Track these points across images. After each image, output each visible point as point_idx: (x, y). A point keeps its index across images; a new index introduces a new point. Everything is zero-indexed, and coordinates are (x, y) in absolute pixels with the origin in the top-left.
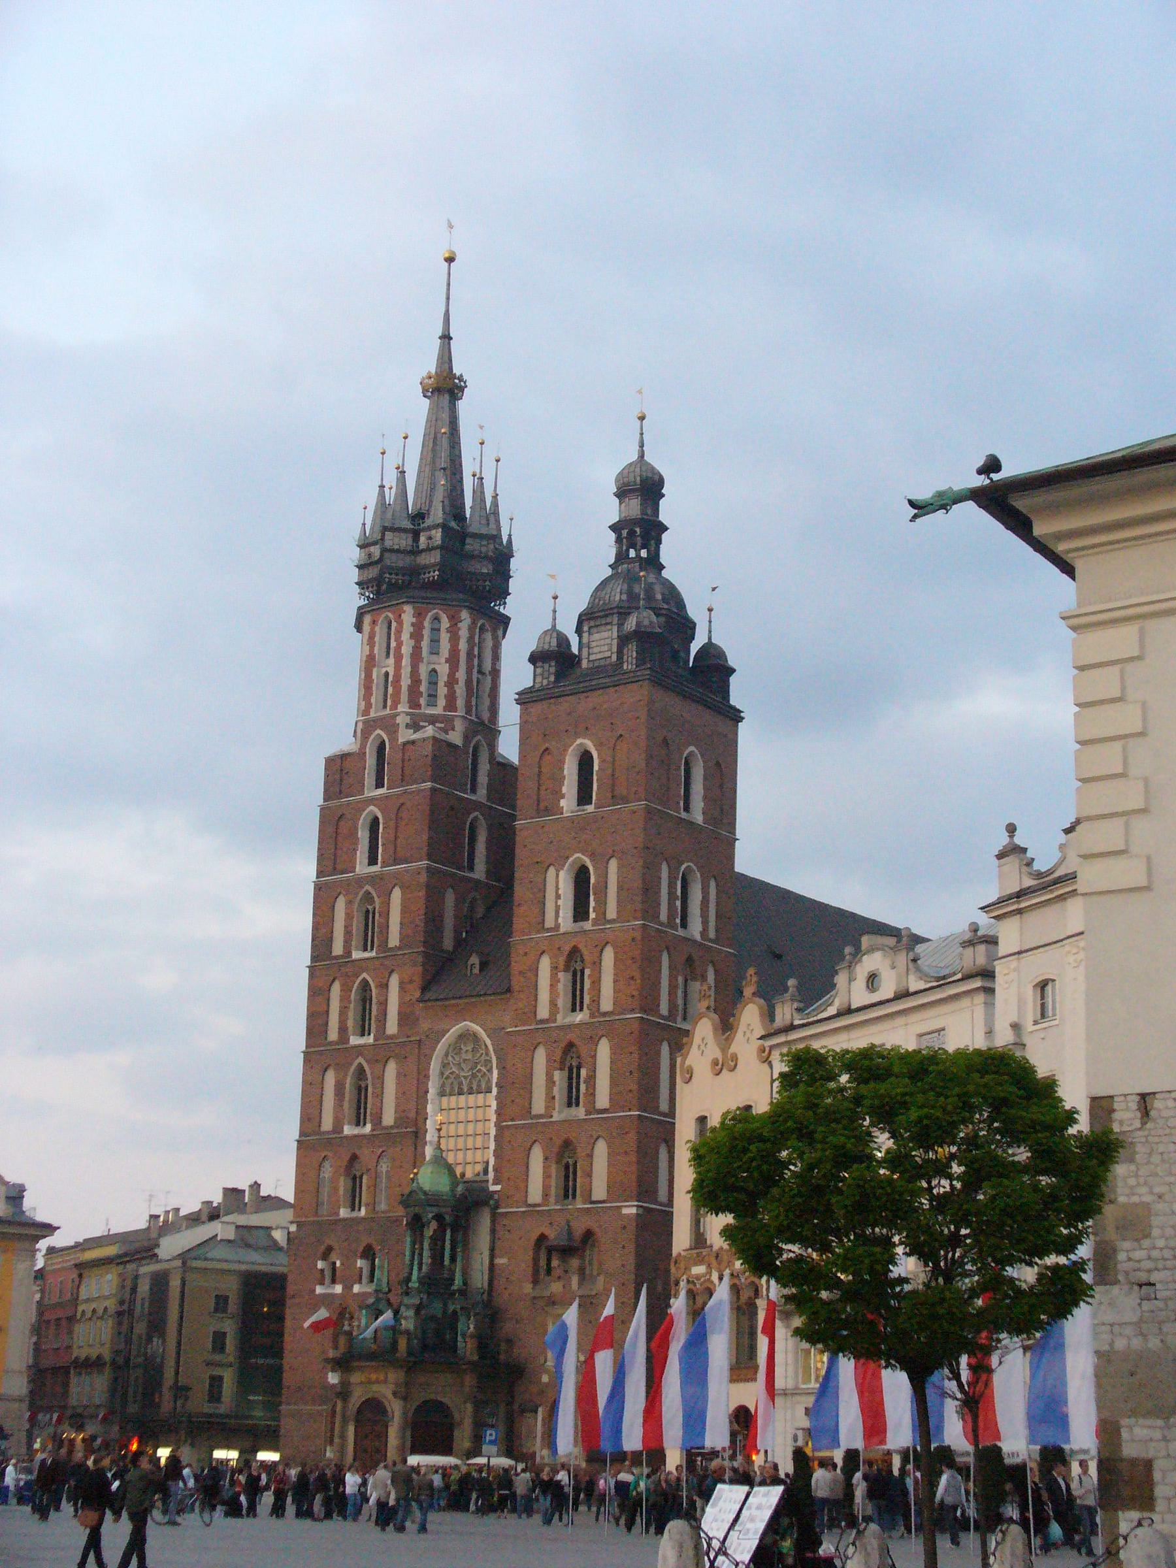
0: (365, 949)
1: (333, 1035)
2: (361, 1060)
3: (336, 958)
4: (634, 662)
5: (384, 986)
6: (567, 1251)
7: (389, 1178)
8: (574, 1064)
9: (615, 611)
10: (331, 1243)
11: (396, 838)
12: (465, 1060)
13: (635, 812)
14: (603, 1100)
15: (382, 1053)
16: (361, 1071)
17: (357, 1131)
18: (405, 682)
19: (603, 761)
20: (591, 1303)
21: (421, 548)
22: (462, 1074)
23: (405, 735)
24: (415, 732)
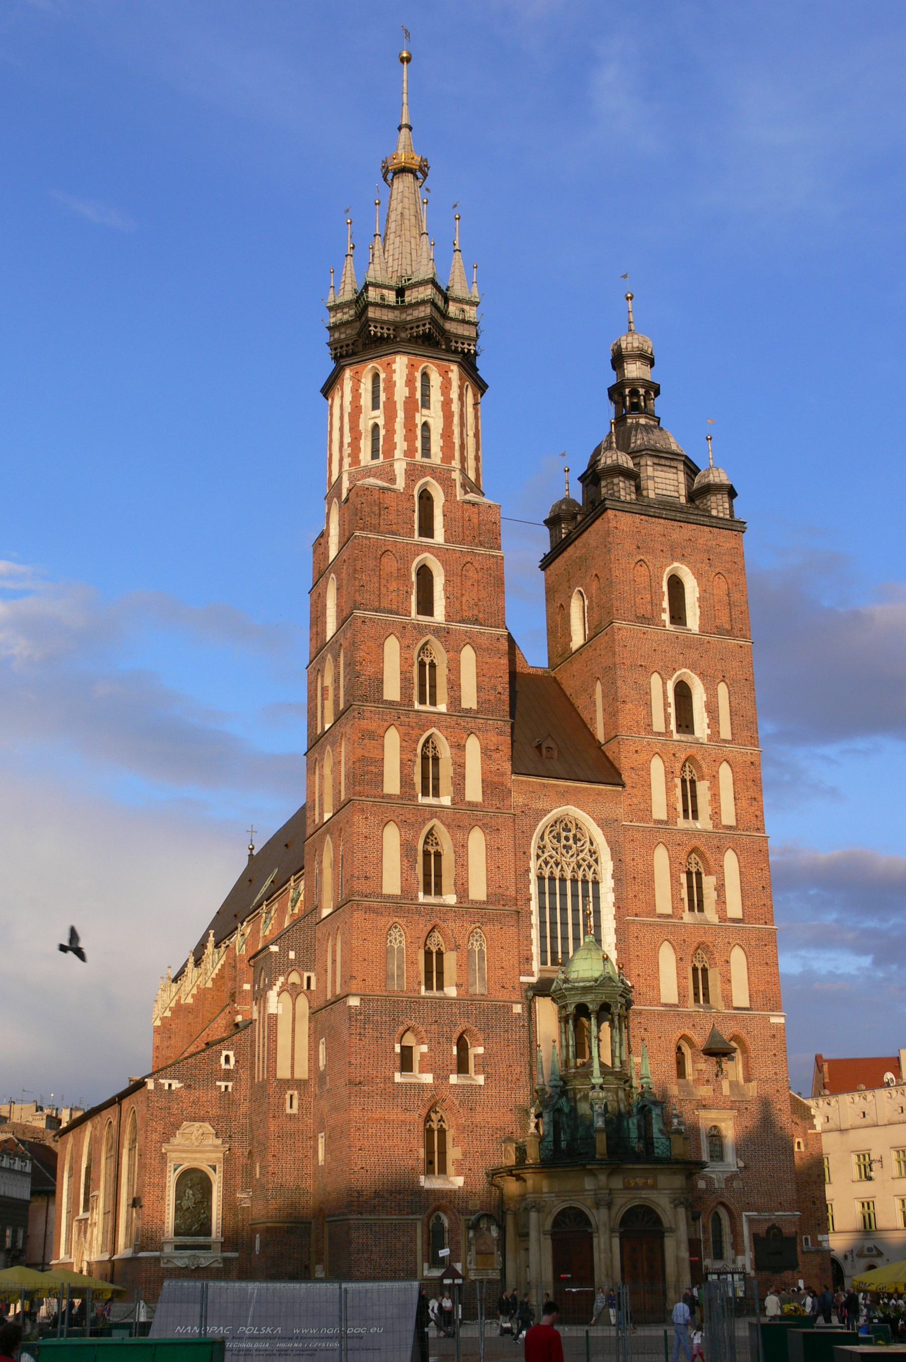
0: (422, 701)
1: (392, 785)
2: (435, 821)
3: (391, 703)
5: (459, 747)
7: (482, 959)
8: (694, 870)
9: (683, 458)
12: (565, 847)
13: (741, 647)
14: (734, 909)
18: (457, 440)
19: (703, 591)
20: (746, 1108)
21: (452, 315)
22: (563, 859)
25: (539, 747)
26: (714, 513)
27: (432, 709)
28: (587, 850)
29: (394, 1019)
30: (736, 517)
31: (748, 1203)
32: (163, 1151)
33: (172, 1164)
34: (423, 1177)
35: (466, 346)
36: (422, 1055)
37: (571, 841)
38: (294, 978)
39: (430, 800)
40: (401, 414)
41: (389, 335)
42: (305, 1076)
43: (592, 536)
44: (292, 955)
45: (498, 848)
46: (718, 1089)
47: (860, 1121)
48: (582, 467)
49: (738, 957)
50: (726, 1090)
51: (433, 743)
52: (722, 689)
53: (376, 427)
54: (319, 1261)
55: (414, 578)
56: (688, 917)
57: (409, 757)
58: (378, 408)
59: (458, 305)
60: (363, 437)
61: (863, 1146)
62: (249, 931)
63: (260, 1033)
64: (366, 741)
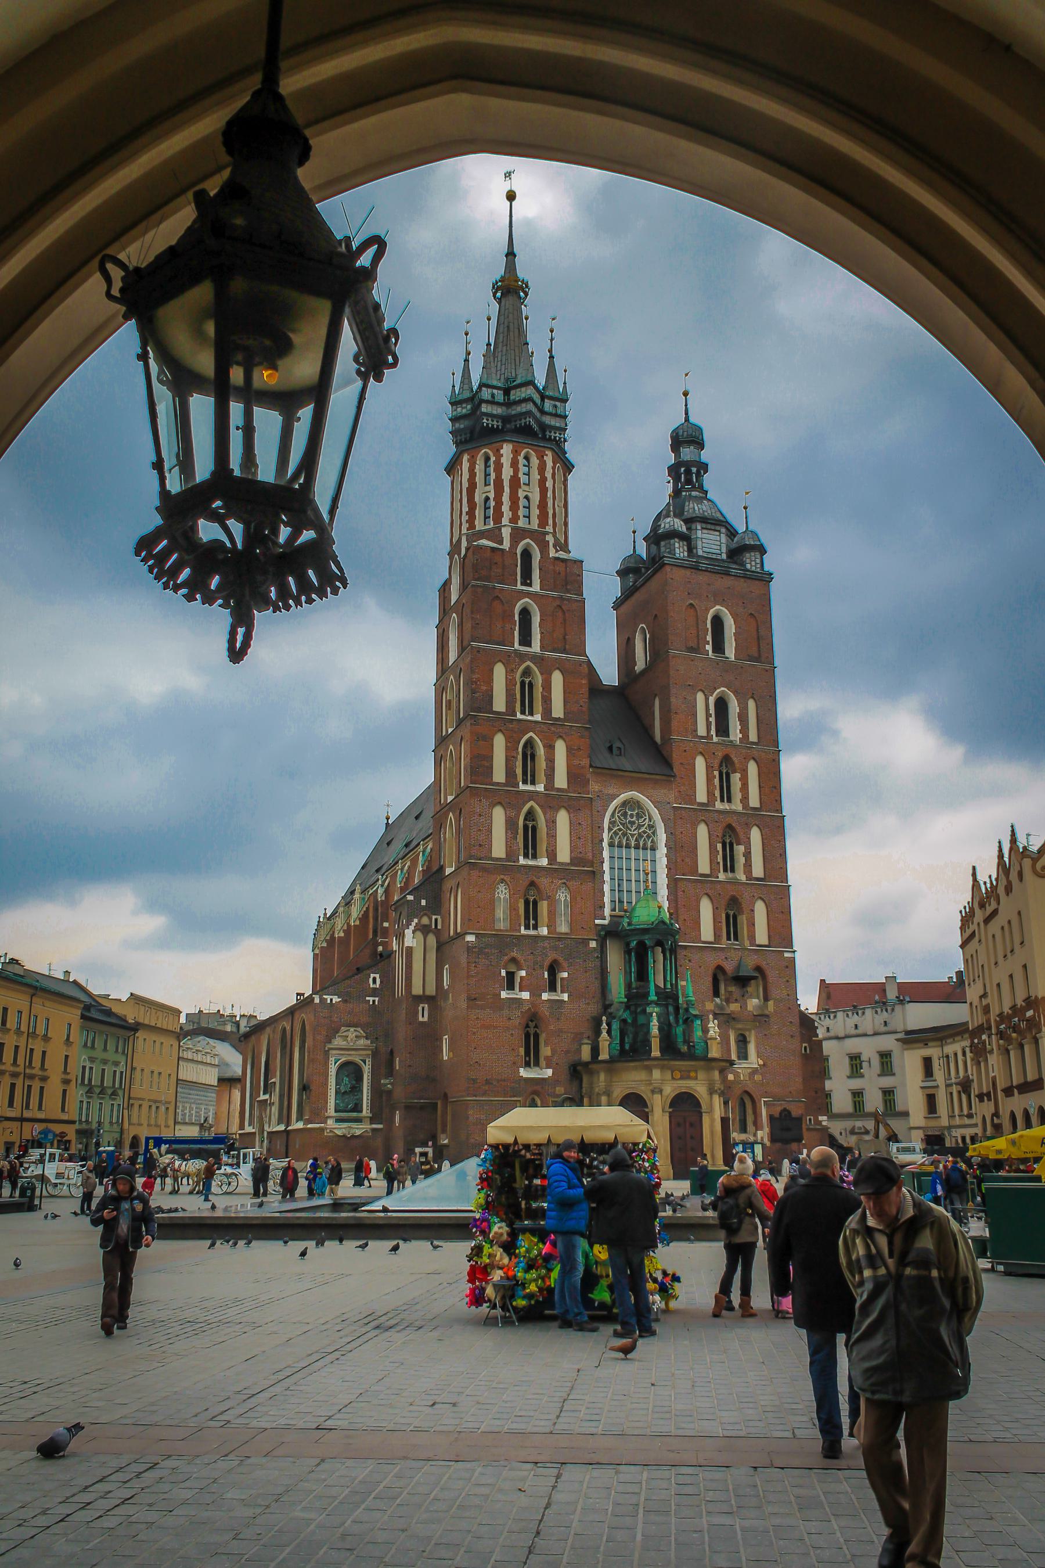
0: (523, 712)
1: (499, 775)
2: (531, 803)
4: (758, 566)
5: (550, 748)
6: (742, 981)
7: (566, 906)
8: (728, 841)
10: (514, 954)
11: (554, 631)
13: (767, 671)
15: (552, 801)
16: (530, 815)
17: (530, 862)
20: (765, 1021)
23: (552, 553)
24: (556, 552)
25: (610, 749)
26: (748, 566)
27: (530, 718)
28: (646, 825)
29: (500, 951)
30: (766, 569)
31: (766, 1092)
32: (326, 1049)
33: (333, 1059)
34: (522, 1069)
35: (557, 435)
36: (521, 977)
37: (634, 819)
38: (425, 921)
39: (529, 787)
40: (507, 489)
41: (498, 426)
42: (434, 993)
43: (654, 584)
44: (423, 902)
45: (580, 824)
46: (744, 1006)
47: (853, 1032)
48: (646, 529)
49: (760, 908)
50: (750, 1008)
51: (531, 744)
52: (751, 704)
53: (487, 499)
54: (444, 1131)
55: (517, 618)
56: (722, 876)
57: (513, 754)
58: (490, 485)
59: (551, 402)
60: (477, 508)
61: (855, 1051)
62: (386, 884)
63: (399, 963)
64: (481, 742)
